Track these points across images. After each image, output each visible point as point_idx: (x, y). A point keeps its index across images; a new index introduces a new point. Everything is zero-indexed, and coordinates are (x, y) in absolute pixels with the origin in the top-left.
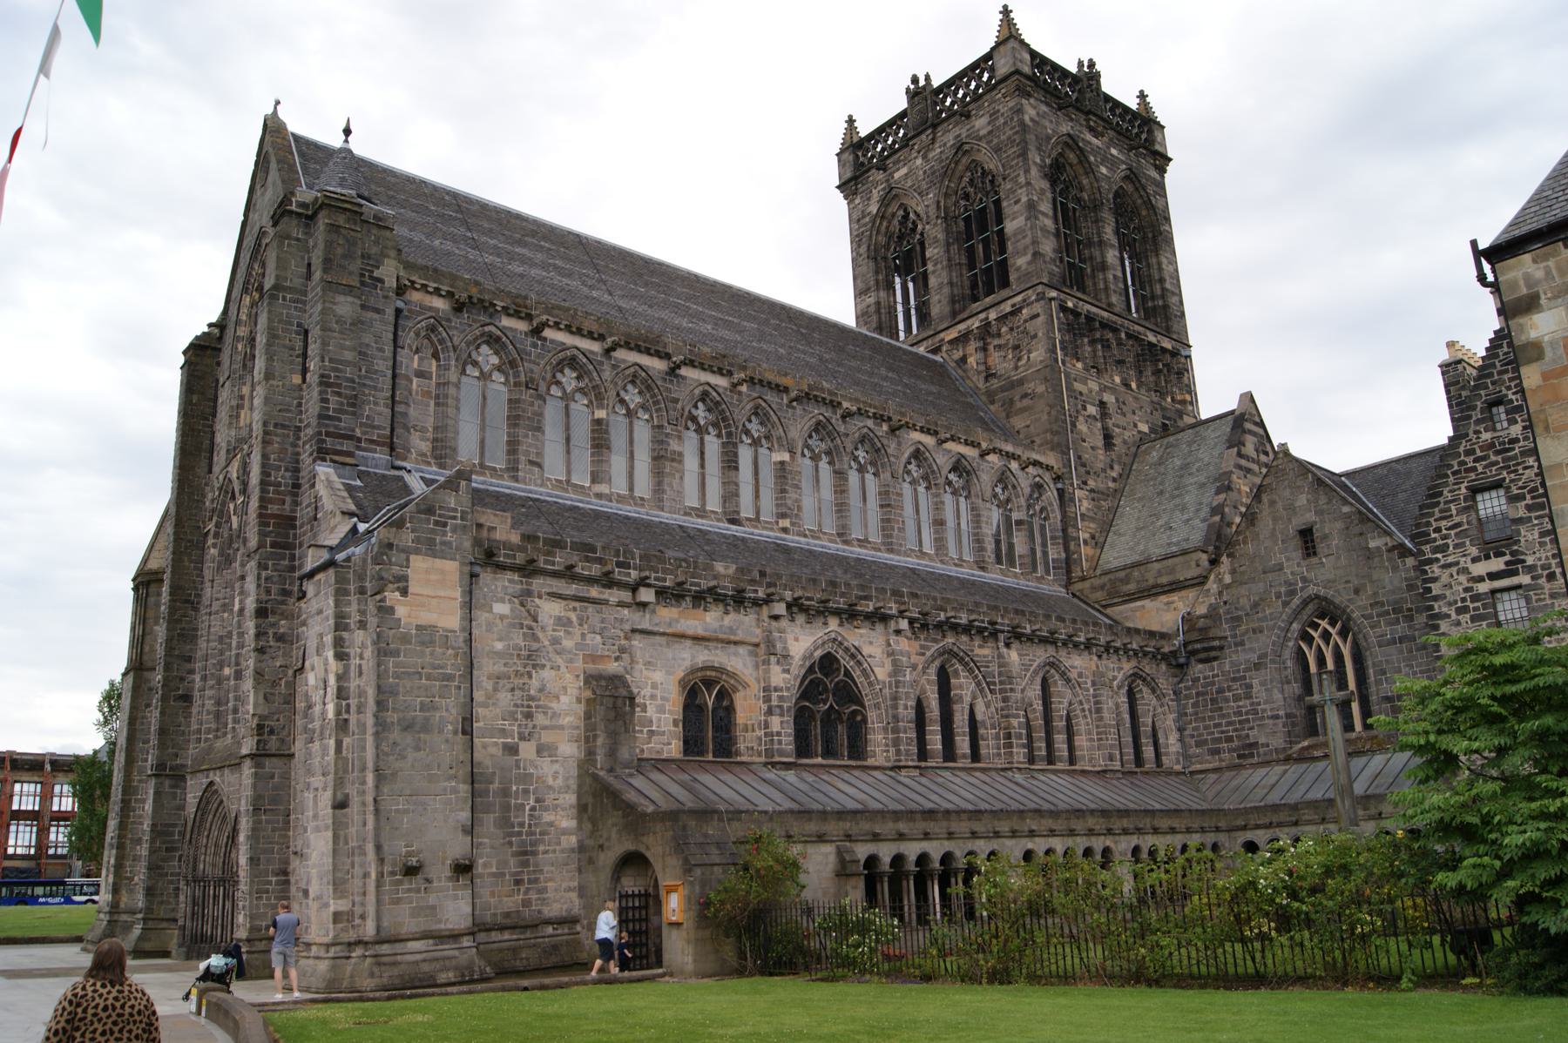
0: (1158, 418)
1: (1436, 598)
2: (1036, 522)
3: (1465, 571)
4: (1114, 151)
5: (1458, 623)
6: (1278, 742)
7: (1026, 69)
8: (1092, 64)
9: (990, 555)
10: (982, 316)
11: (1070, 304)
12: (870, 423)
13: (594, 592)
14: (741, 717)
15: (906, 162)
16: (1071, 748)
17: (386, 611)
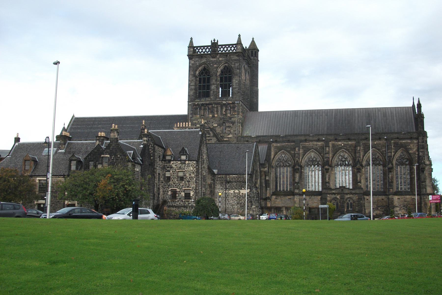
4: (220, 59)
8: (214, 40)
11: (196, 104)
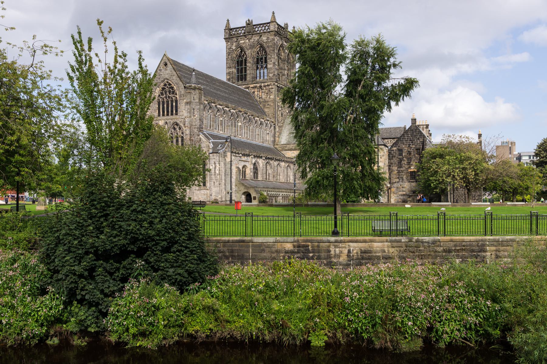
14: (247, 172)
17: (225, 160)
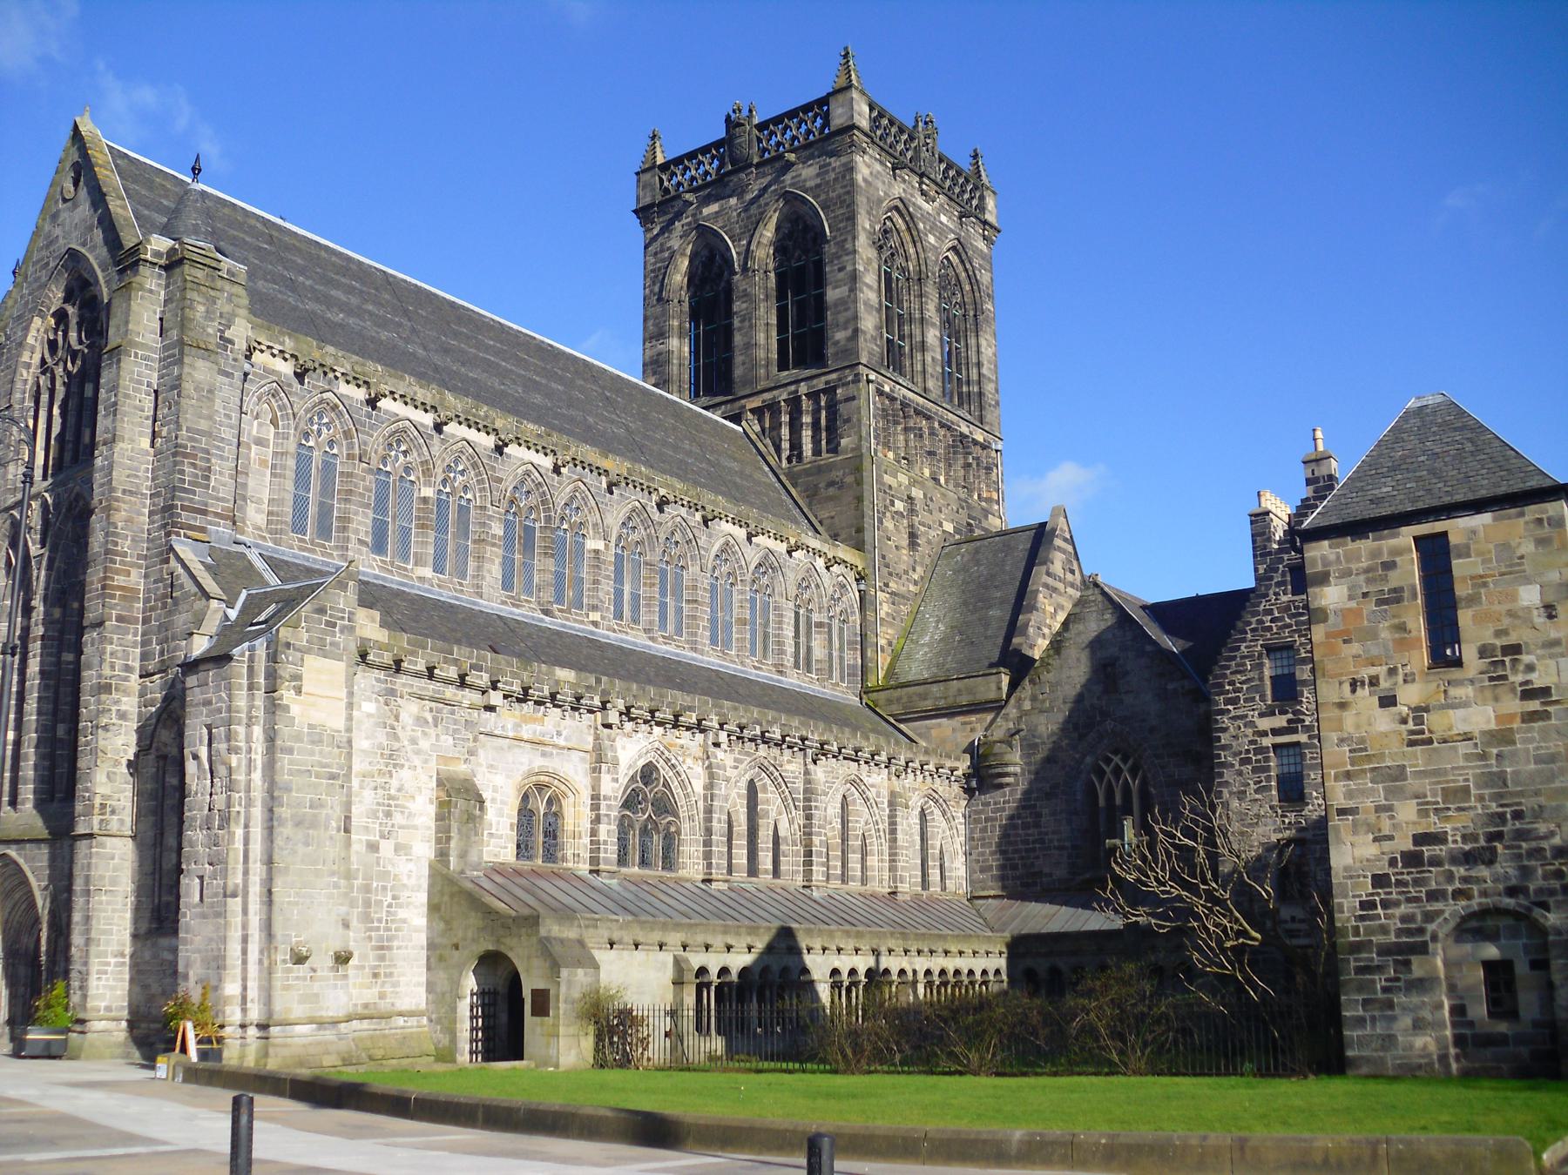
0: (963, 517)
1: (1224, 748)
2: (836, 624)
3: (1252, 724)
4: (944, 219)
5: (1240, 773)
6: (1060, 873)
7: (864, 123)
9: (789, 660)
10: (793, 388)
11: (887, 389)
12: (683, 511)
13: (450, 692)
14: (569, 823)
15: (718, 198)
16: (864, 868)
